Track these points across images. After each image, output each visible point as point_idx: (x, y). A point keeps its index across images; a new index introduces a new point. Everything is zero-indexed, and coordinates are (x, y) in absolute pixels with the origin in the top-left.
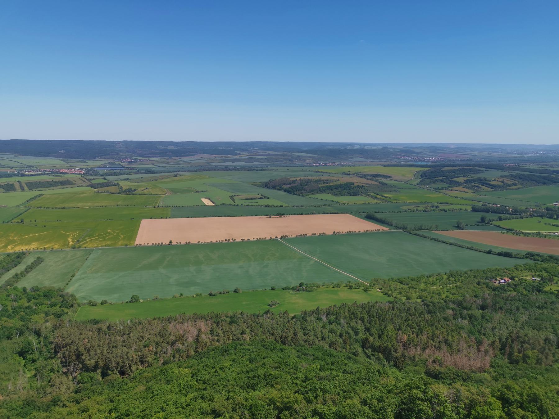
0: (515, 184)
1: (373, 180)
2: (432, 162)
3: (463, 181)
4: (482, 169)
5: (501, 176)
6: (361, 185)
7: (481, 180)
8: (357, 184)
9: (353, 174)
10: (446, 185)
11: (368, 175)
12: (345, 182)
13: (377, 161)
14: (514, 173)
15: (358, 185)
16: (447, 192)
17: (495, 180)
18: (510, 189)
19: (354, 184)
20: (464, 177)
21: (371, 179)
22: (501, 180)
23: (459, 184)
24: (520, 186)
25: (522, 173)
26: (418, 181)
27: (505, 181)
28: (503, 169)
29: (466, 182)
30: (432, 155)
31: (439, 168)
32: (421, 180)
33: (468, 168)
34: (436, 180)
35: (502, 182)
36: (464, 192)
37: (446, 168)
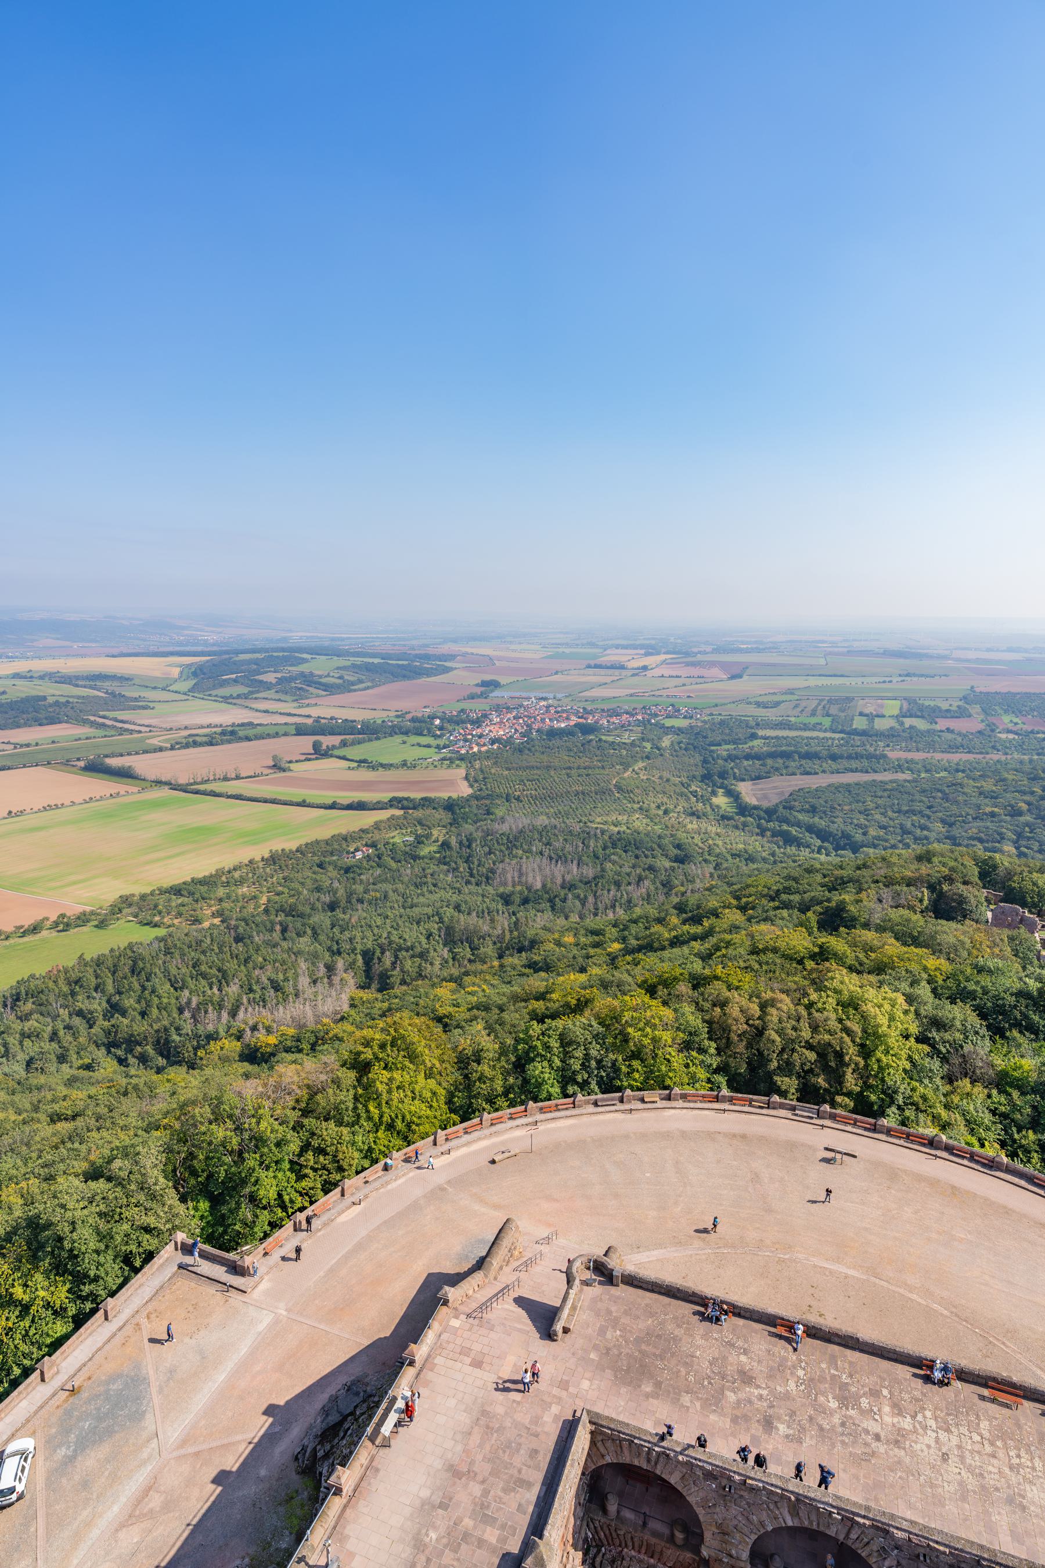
0: (361, 681)
1: (91, 687)
2: (213, 645)
3: (274, 681)
4: (305, 656)
5: (338, 668)
6: (63, 700)
7: (305, 676)
8: (54, 699)
9: (41, 678)
10: (246, 690)
11: (77, 678)
12: (23, 695)
13: (94, 645)
14: (359, 660)
15: (57, 701)
16: (248, 703)
17: (328, 676)
18: (355, 690)
19: (44, 698)
20: (275, 672)
21: (85, 687)
22: (337, 675)
23: (268, 686)
24: (369, 684)
25: (370, 660)
26: (191, 683)
27: (346, 677)
28: (339, 653)
29: (280, 681)
30: (212, 632)
31: (227, 656)
32: (194, 682)
33: (281, 654)
34: (225, 680)
35: (340, 678)
36: (279, 700)
37: (242, 657)
